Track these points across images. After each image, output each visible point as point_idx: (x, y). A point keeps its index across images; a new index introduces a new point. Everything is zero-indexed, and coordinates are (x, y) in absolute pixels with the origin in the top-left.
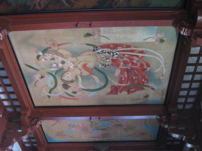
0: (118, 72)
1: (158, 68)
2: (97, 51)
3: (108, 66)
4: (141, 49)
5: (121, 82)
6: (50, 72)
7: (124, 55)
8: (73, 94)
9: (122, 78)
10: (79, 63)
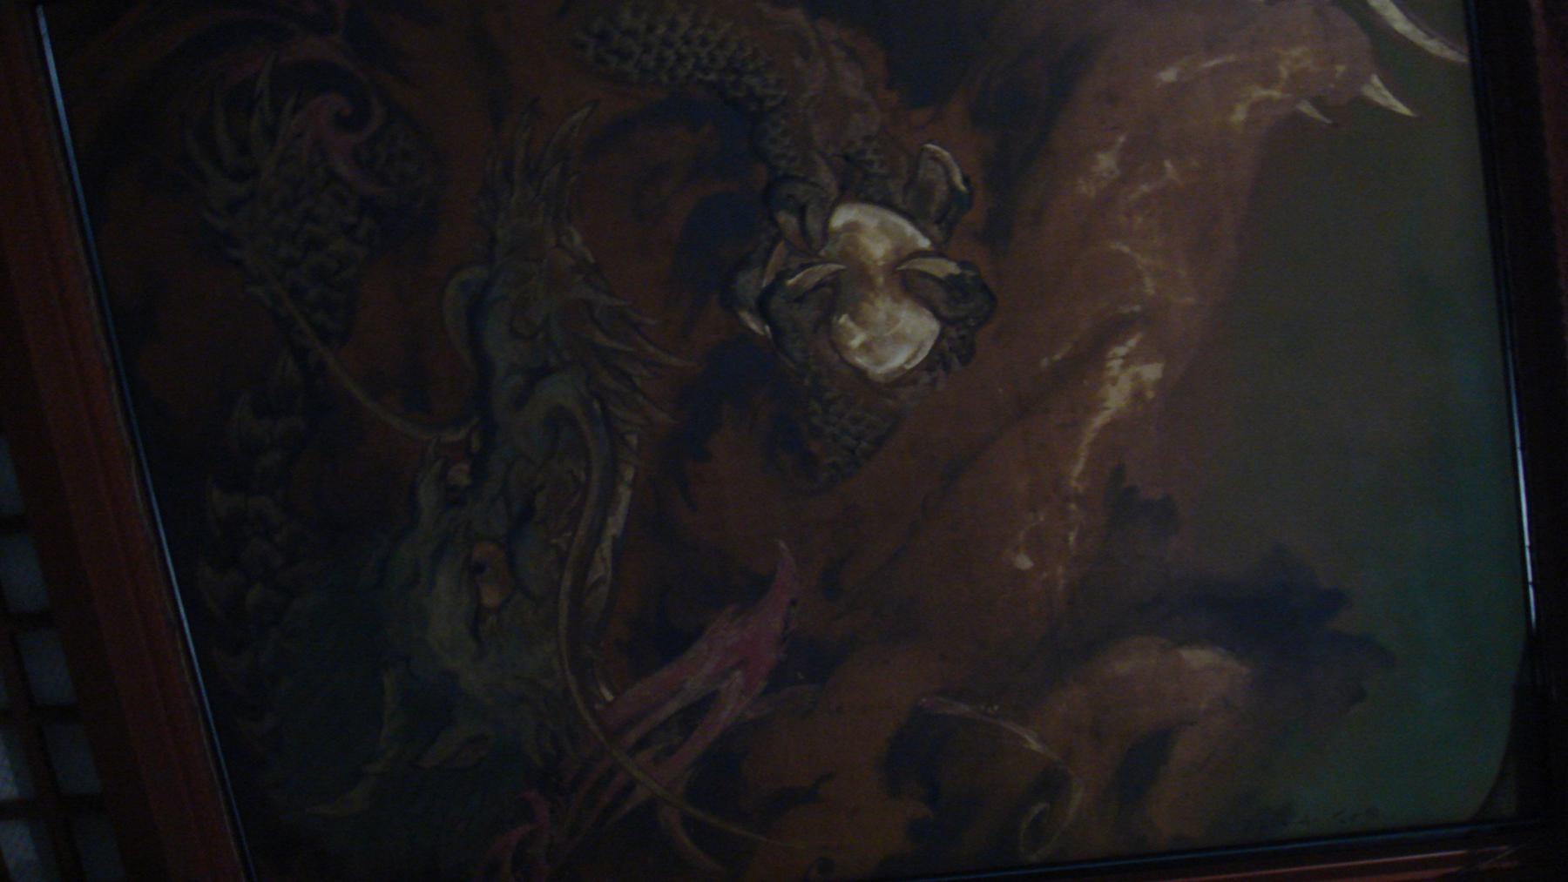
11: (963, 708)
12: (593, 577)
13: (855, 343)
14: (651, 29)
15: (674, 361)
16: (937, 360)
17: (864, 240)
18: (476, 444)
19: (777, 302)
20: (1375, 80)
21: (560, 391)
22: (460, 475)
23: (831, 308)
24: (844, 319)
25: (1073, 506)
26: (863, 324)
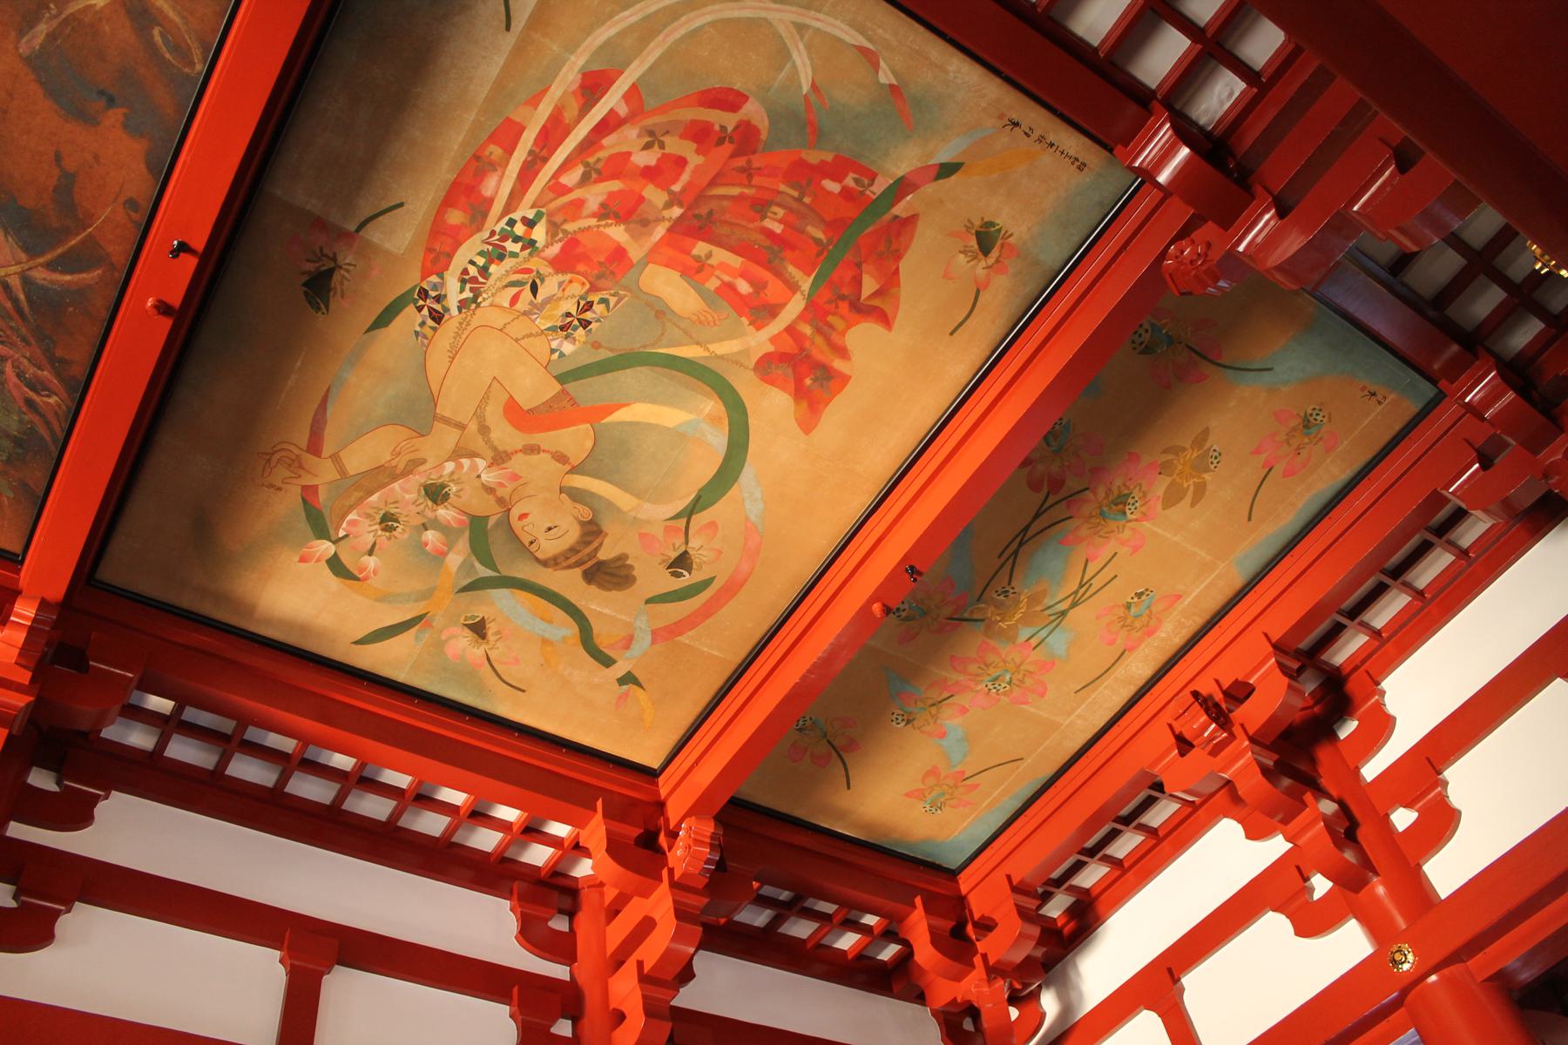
0: (666, 284)
1: (784, 54)
2: (452, 302)
3: (589, 306)
4: (568, 78)
5: (760, 310)
6: (465, 582)
7: (556, 188)
8: (687, 579)
9: (731, 287)
10: (484, 430)
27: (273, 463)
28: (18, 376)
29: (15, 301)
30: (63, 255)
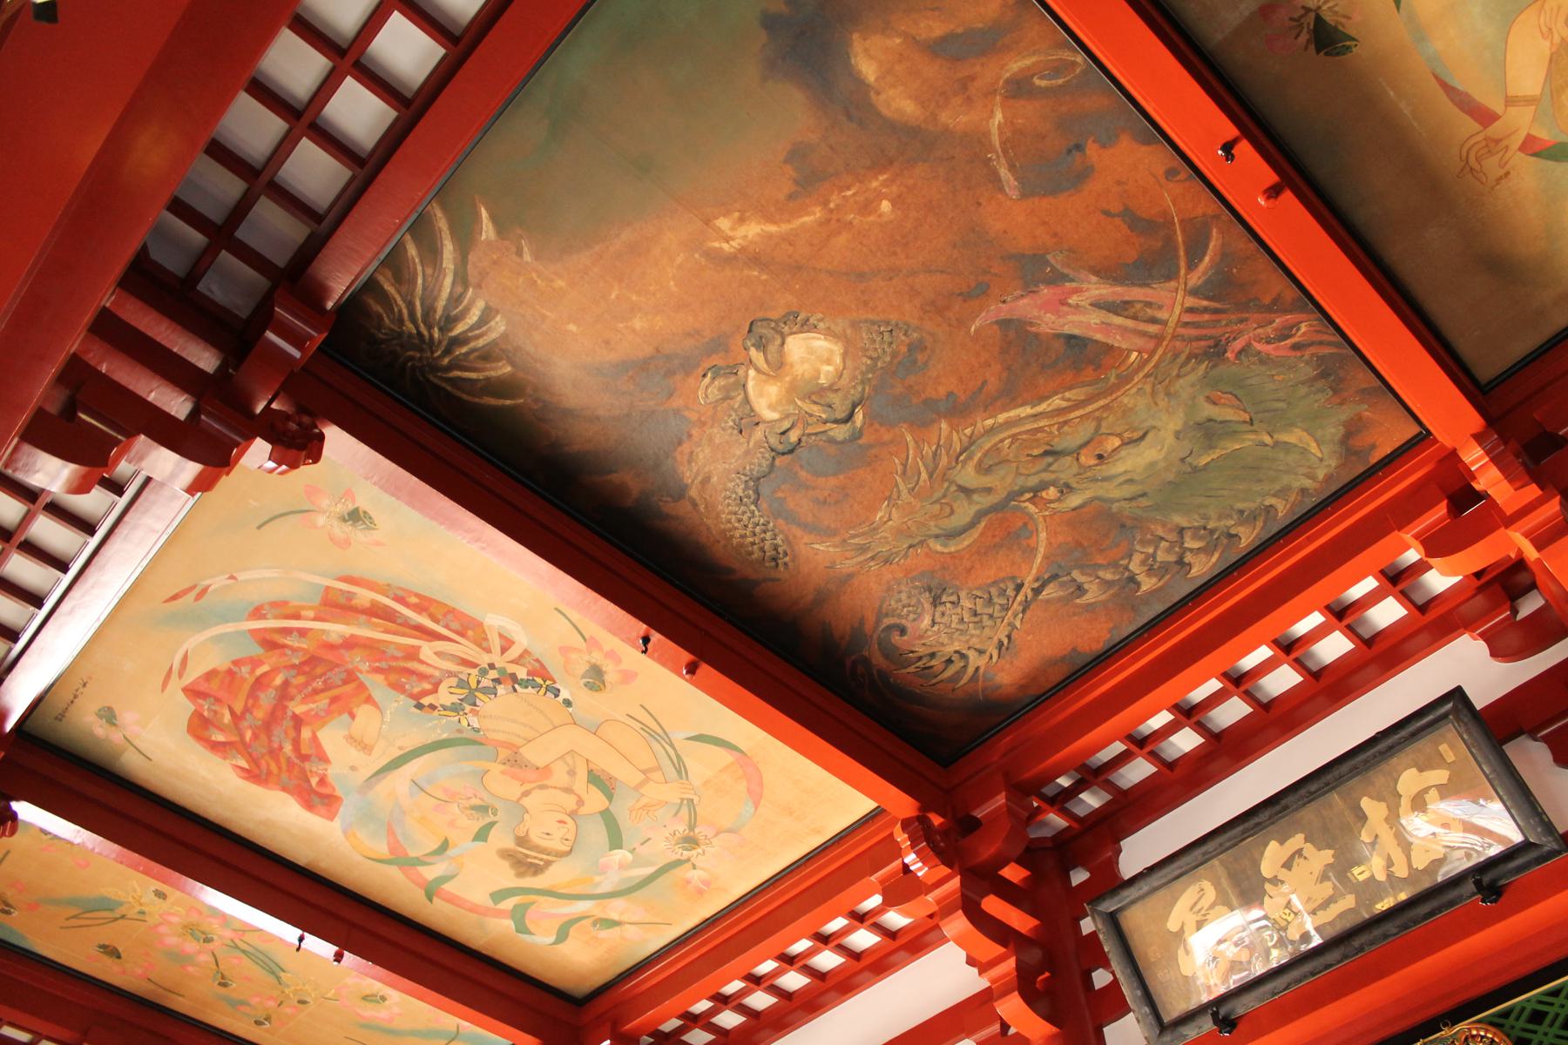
11: (1004, 172)
12: (1064, 404)
13: (830, 368)
14: (753, 544)
15: (909, 438)
16: (806, 326)
17: (774, 398)
18: (1028, 496)
19: (841, 415)
20: (484, 237)
21: (968, 475)
22: (1052, 492)
23: (822, 390)
24: (822, 381)
25: (832, 205)
26: (818, 372)
27: (1477, 167)
28: (1268, 343)
29: (1206, 310)
30: (1187, 253)
